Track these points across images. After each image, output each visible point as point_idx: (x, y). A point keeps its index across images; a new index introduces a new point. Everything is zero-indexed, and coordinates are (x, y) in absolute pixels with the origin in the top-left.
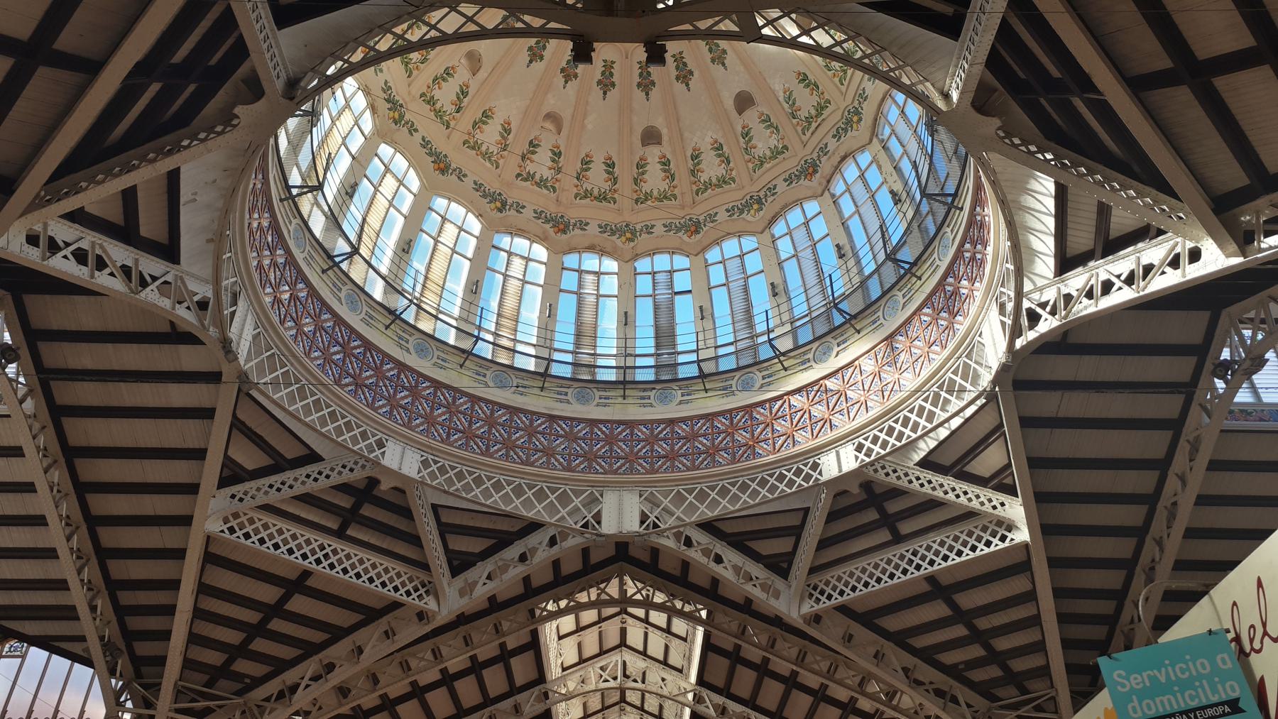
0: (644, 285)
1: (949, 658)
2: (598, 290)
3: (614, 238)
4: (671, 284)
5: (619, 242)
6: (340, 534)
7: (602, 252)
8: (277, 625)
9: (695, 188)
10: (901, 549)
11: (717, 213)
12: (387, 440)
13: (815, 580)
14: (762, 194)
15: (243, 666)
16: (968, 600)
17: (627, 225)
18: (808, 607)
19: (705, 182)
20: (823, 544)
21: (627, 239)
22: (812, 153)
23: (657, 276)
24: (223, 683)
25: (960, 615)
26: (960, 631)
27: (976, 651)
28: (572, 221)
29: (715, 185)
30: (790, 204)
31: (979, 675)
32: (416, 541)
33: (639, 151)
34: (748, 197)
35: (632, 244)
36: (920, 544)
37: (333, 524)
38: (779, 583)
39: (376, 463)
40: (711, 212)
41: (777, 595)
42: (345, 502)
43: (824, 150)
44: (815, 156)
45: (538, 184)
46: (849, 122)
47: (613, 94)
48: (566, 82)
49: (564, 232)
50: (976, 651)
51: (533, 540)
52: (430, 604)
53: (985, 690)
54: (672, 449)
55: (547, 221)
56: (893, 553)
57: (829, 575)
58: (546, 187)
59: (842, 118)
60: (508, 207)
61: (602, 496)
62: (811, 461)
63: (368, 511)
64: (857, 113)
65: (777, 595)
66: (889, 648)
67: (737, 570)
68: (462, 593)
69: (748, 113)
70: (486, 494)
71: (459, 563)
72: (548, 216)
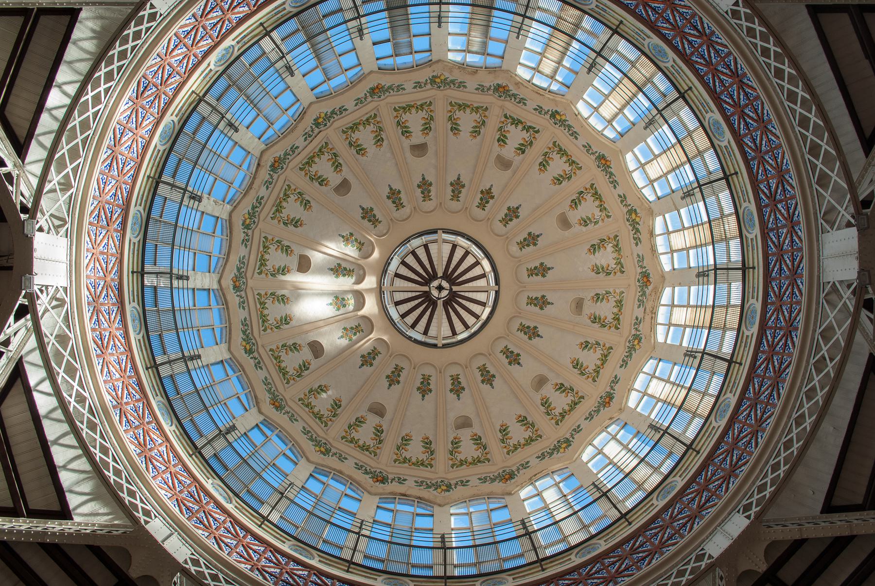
0: (420, 43)
2: (469, 40)
3: (451, 78)
4: (396, 46)
5: (447, 75)
7: (462, 66)
9: (378, 119)
11: (356, 105)
12: (727, 12)
14: (316, 130)
17: (439, 87)
19: (369, 125)
21: (439, 77)
22: (279, 176)
23: (408, 50)
28: (491, 92)
29: (360, 124)
30: (289, 133)
33: (429, 139)
34: (328, 124)
35: (435, 74)
40: (361, 105)
43: (268, 184)
44: (275, 176)
45: (520, 122)
46: (252, 215)
47: (452, 178)
48: (490, 189)
49: (499, 86)
55: (514, 96)
58: (513, 119)
59: (259, 215)
60: (550, 113)
64: (247, 227)
69: (338, 181)
72: (513, 99)
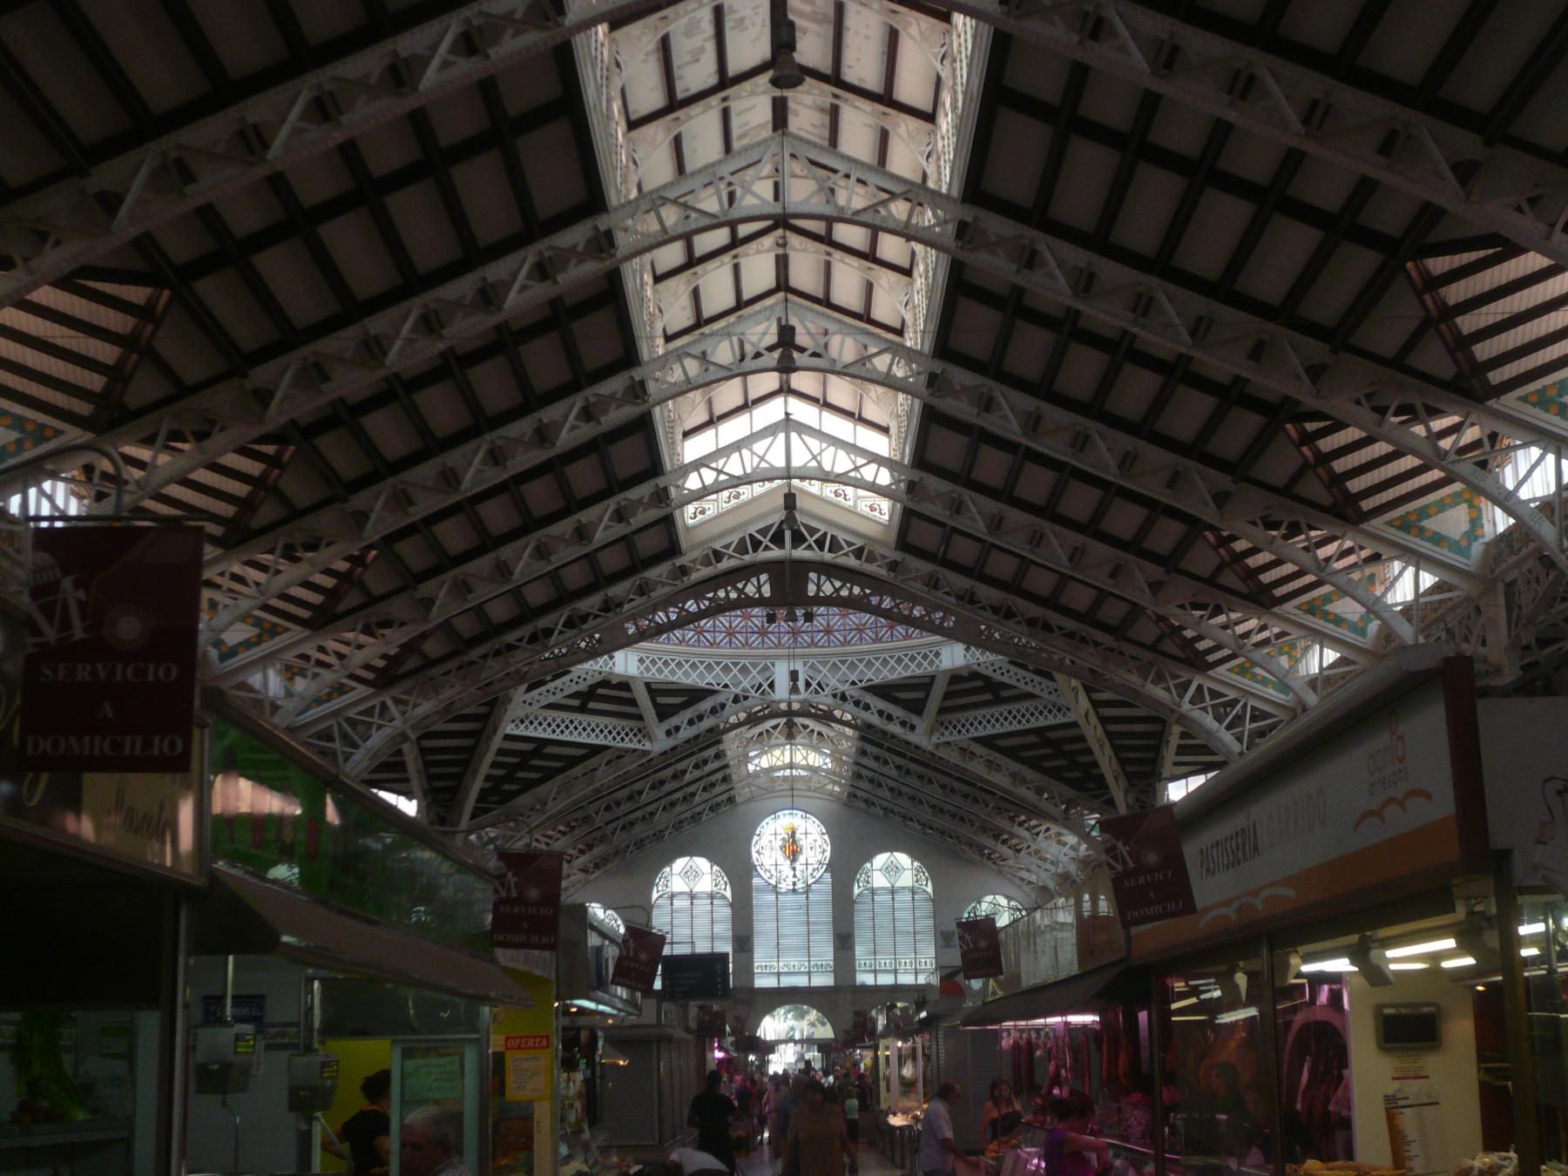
1: (1047, 764)
6: (582, 709)
8: (534, 762)
10: (1004, 708)
13: (943, 718)
15: (507, 787)
16: (1052, 735)
18: (934, 739)
20: (948, 695)
24: (495, 798)
25: (1047, 742)
26: (1048, 751)
27: (1063, 762)
31: (1069, 775)
32: (633, 702)
36: (1013, 707)
37: (576, 703)
38: (915, 720)
39: (611, 673)
41: (913, 728)
42: (586, 690)
50: (1063, 762)
51: (719, 699)
52: (648, 746)
53: (1071, 783)
54: (828, 625)
56: (996, 710)
57: (949, 717)
61: (773, 665)
62: (935, 649)
63: (600, 691)
65: (913, 728)
66: (998, 758)
67: (880, 713)
68: (668, 733)
70: (686, 674)
71: (664, 713)
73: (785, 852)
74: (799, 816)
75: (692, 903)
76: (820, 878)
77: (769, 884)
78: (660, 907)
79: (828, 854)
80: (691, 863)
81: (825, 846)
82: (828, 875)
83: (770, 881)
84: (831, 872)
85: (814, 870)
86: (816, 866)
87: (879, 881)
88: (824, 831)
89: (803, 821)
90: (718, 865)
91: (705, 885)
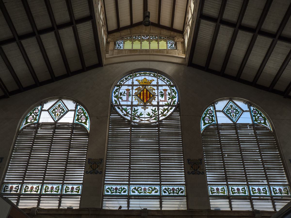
73: (140, 97)
74: (152, 75)
75: (54, 132)
76: (171, 115)
77: (125, 119)
78: (26, 134)
79: (176, 99)
80: (59, 103)
81: (173, 94)
82: (177, 114)
83: (126, 117)
84: (179, 111)
85: (165, 110)
86: (166, 107)
87: (222, 119)
88: (172, 84)
89: (155, 79)
90: (82, 105)
91: (68, 118)
